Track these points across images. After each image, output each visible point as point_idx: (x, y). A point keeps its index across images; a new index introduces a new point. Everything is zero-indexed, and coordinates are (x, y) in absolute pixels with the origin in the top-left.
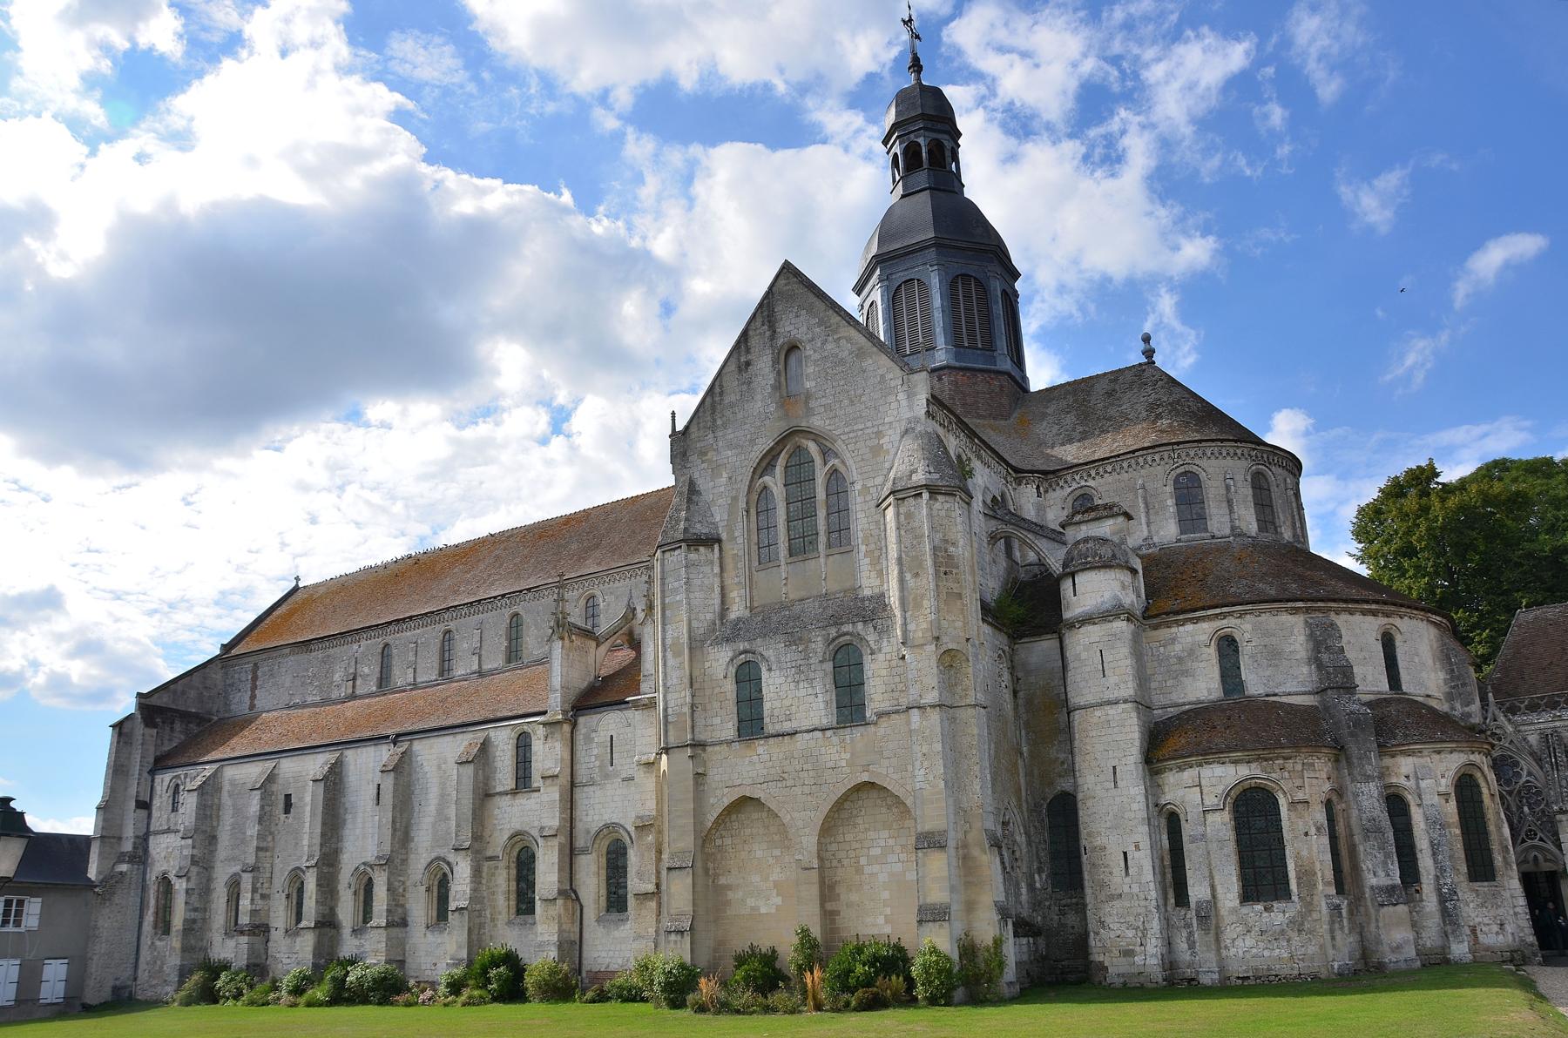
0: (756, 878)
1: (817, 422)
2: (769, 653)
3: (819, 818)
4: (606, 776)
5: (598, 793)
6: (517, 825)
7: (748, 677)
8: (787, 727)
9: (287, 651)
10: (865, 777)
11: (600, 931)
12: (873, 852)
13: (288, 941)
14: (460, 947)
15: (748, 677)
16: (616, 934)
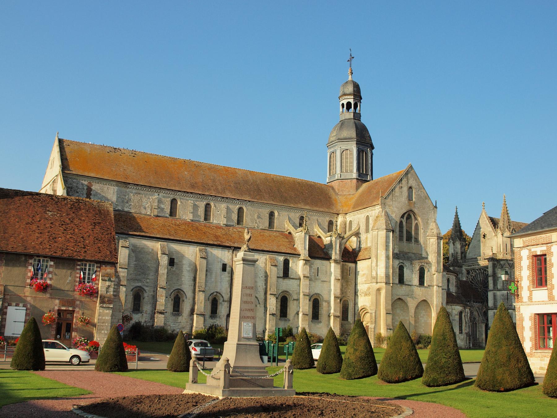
0: (397, 318)
1: (416, 211)
2: (407, 265)
3: (415, 306)
4: (316, 279)
5: (313, 284)
6: (284, 288)
7: (401, 268)
8: (410, 283)
9: (114, 183)
10: (424, 299)
11: (313, 325)
12: (422, 315)
13: (174, 318)
14: (272, 326)
15: (401, 268)
16: (318, 326)
